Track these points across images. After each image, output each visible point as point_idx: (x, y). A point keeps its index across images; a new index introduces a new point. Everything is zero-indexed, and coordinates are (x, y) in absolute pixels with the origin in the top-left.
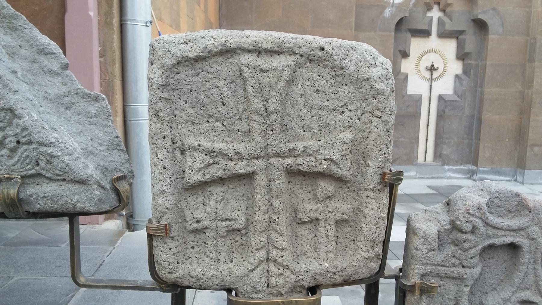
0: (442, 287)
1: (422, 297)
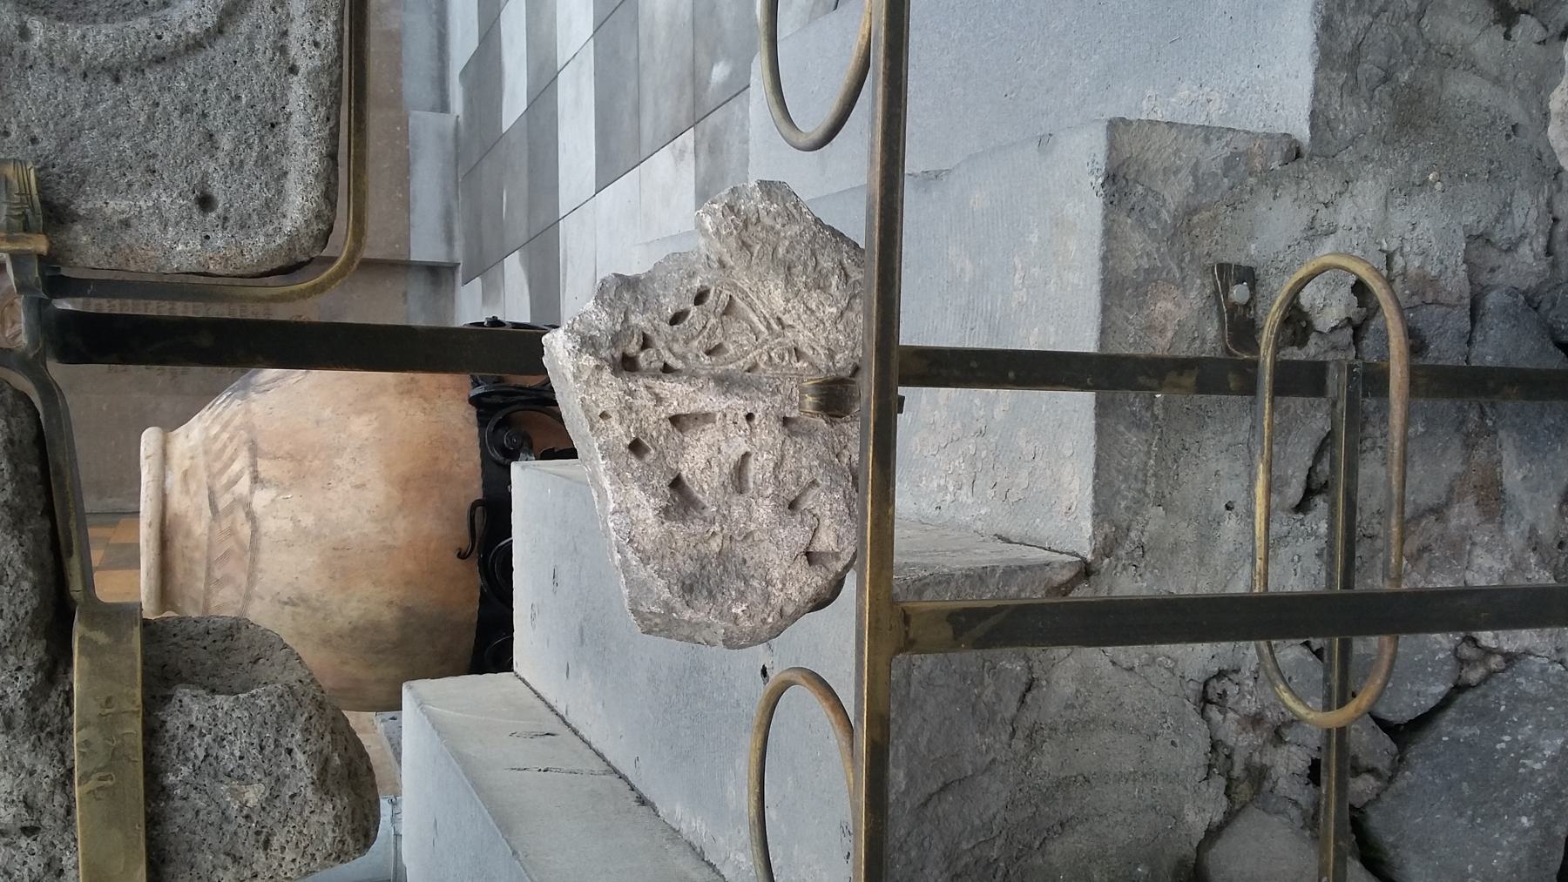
0: (37, 131)
1: (82, 212)
